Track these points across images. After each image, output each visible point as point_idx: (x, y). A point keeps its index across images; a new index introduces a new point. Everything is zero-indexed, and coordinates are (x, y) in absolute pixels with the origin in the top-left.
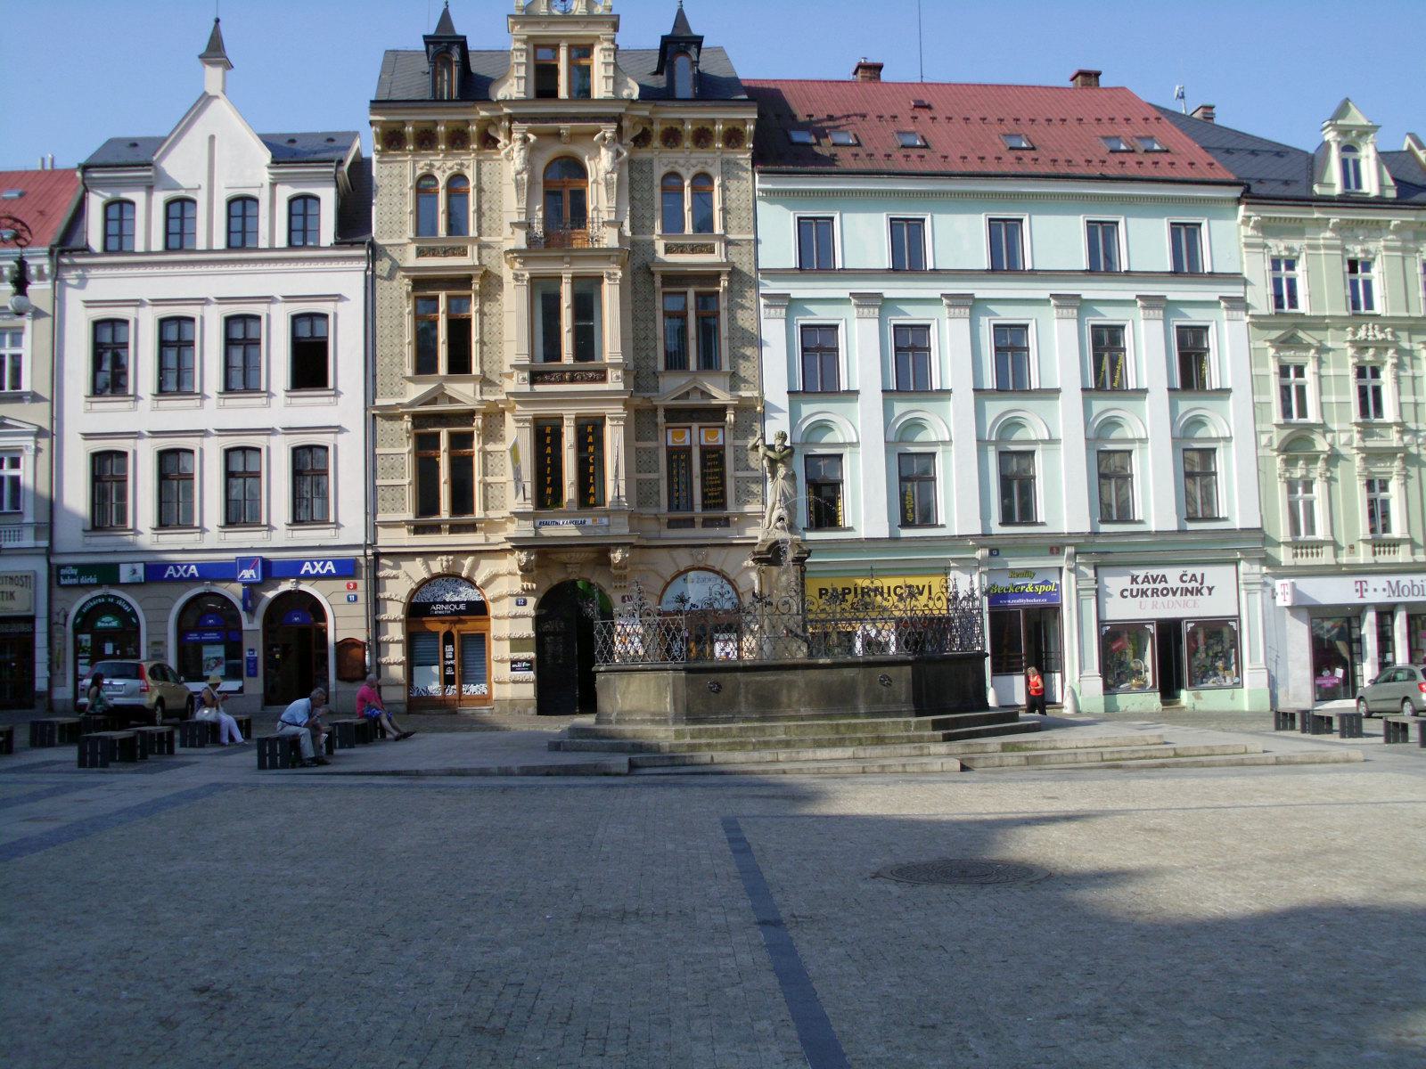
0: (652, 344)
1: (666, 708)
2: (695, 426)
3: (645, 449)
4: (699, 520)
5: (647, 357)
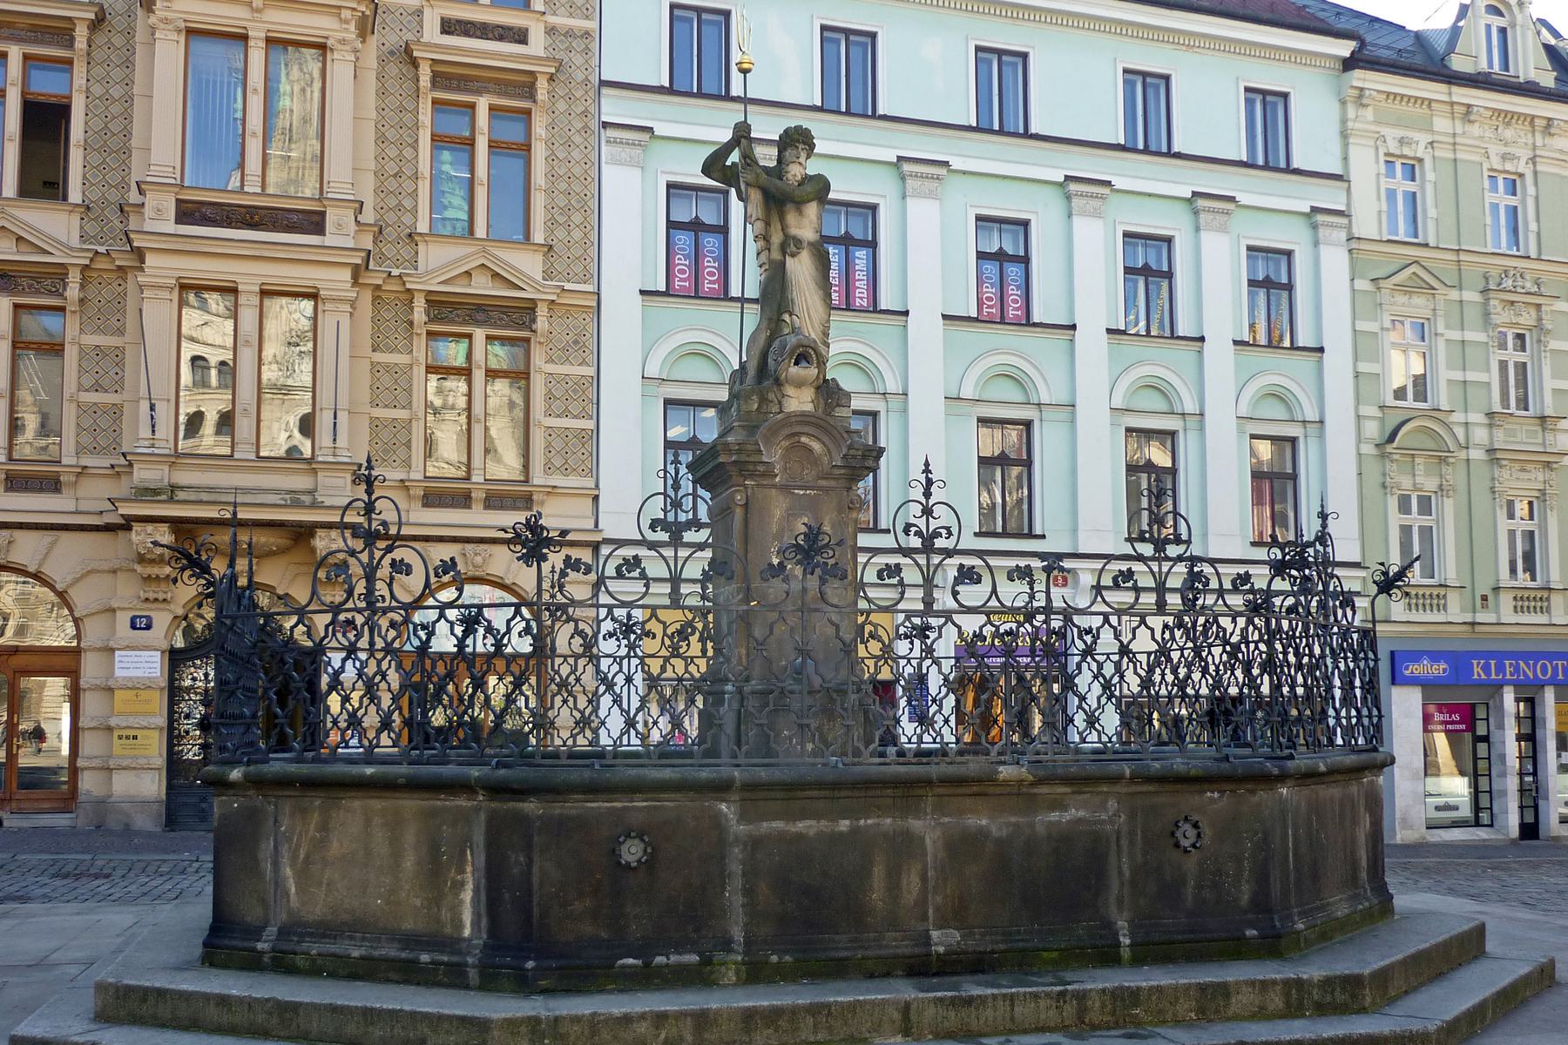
0: (408, 186)
1: (459, 925)
2: (479, 334)
3: (388, 368)
4: (478, 495)
5: (400, 206)
